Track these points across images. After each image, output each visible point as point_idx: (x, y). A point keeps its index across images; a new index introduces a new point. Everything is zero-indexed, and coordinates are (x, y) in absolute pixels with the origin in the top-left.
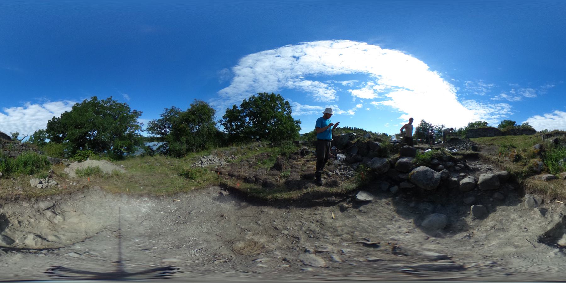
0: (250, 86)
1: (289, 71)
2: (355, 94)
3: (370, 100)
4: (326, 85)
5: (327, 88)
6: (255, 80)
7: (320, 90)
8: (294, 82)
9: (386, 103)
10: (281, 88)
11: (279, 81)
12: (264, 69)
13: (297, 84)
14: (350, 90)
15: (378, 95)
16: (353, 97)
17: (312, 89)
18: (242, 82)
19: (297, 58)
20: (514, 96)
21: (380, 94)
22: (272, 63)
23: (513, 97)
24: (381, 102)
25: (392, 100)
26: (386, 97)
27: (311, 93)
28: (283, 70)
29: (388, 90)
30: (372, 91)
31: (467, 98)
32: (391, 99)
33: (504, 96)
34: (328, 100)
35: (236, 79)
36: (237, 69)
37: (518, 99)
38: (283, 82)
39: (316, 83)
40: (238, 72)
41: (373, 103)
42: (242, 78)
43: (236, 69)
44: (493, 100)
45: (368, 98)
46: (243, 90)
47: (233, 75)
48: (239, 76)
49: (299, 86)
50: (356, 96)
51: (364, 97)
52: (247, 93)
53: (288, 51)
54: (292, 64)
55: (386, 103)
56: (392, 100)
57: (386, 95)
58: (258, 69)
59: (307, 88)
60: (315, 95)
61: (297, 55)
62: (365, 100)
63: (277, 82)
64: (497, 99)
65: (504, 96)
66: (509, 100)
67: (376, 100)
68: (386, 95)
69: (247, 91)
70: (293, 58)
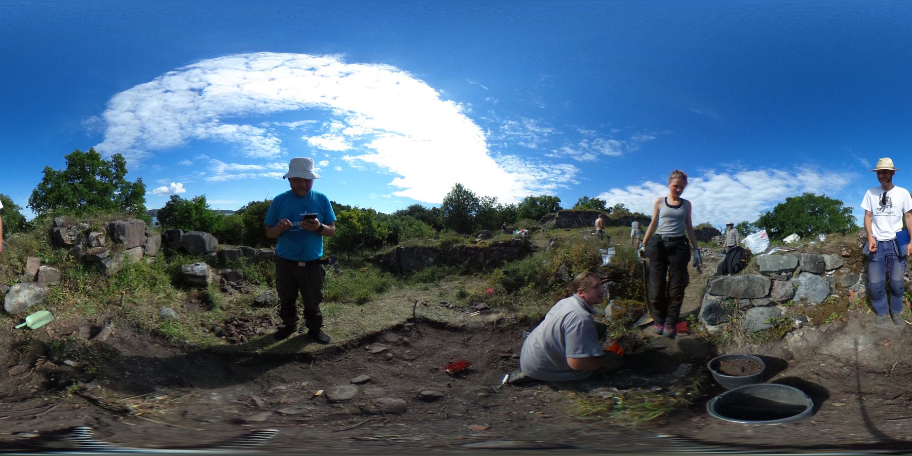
0: (138, 139)
1: (194, 111)
2: (314, 144)
3: (340, 153)
4: (262, 131)
5: (265, 136)
6: (143, 130)
7: (254, 139)
8: (207, 128)
9: (368, 158)
10: (188, 139)
11: (182, 128)
12: (153, 112)
13: (213, 132)
14: (305, 138)
15: (353, 146)
16: (311, 148)
17: (240, 138)
18: (123, 135)
19: (200, 91)
20: (585, 151)
21: (356, 144)
22: (162, 103)
23: (583, 154)
24: (359, 157)
25: (377, 153)
26: (366, 148)
27: (239, 144)
28: (183, 111)
29: (368, 138)
30: (342, 138)
31: (505, 152)
32: (375, 151)
33: (569, 151)
34: (269, 154)
35: (113, 130)
36: (109, 115)
37: (589, 157)
38: (190, 129)
39: (245, 128)
40: (114, 119)
41: (346, 158)
42: (122, 129)
43: (109, 115)
44: (548, 158)
45: (336, 149)
46: (127, 145)
47: (105, 124)
48: (115, 125)
49: (217, 135)
50: (316, 147)
51: (330, 148)
52: (134, 150)
53: (177, 81)
54: (193, 101)
55: (368, 158)
56: (377, 153)
57: (366, 145)
58: (145, 113)
59: (231, 137)
60: (247, 148)
61: (196, 86)
62: (332, 153)
63: (178, 131)
64: (557, 156)
65: (569, 151)
66: (577, 158)
67: (350, 153)
68: (366, 145)
69: (133, 147)
70: (191, 93)
